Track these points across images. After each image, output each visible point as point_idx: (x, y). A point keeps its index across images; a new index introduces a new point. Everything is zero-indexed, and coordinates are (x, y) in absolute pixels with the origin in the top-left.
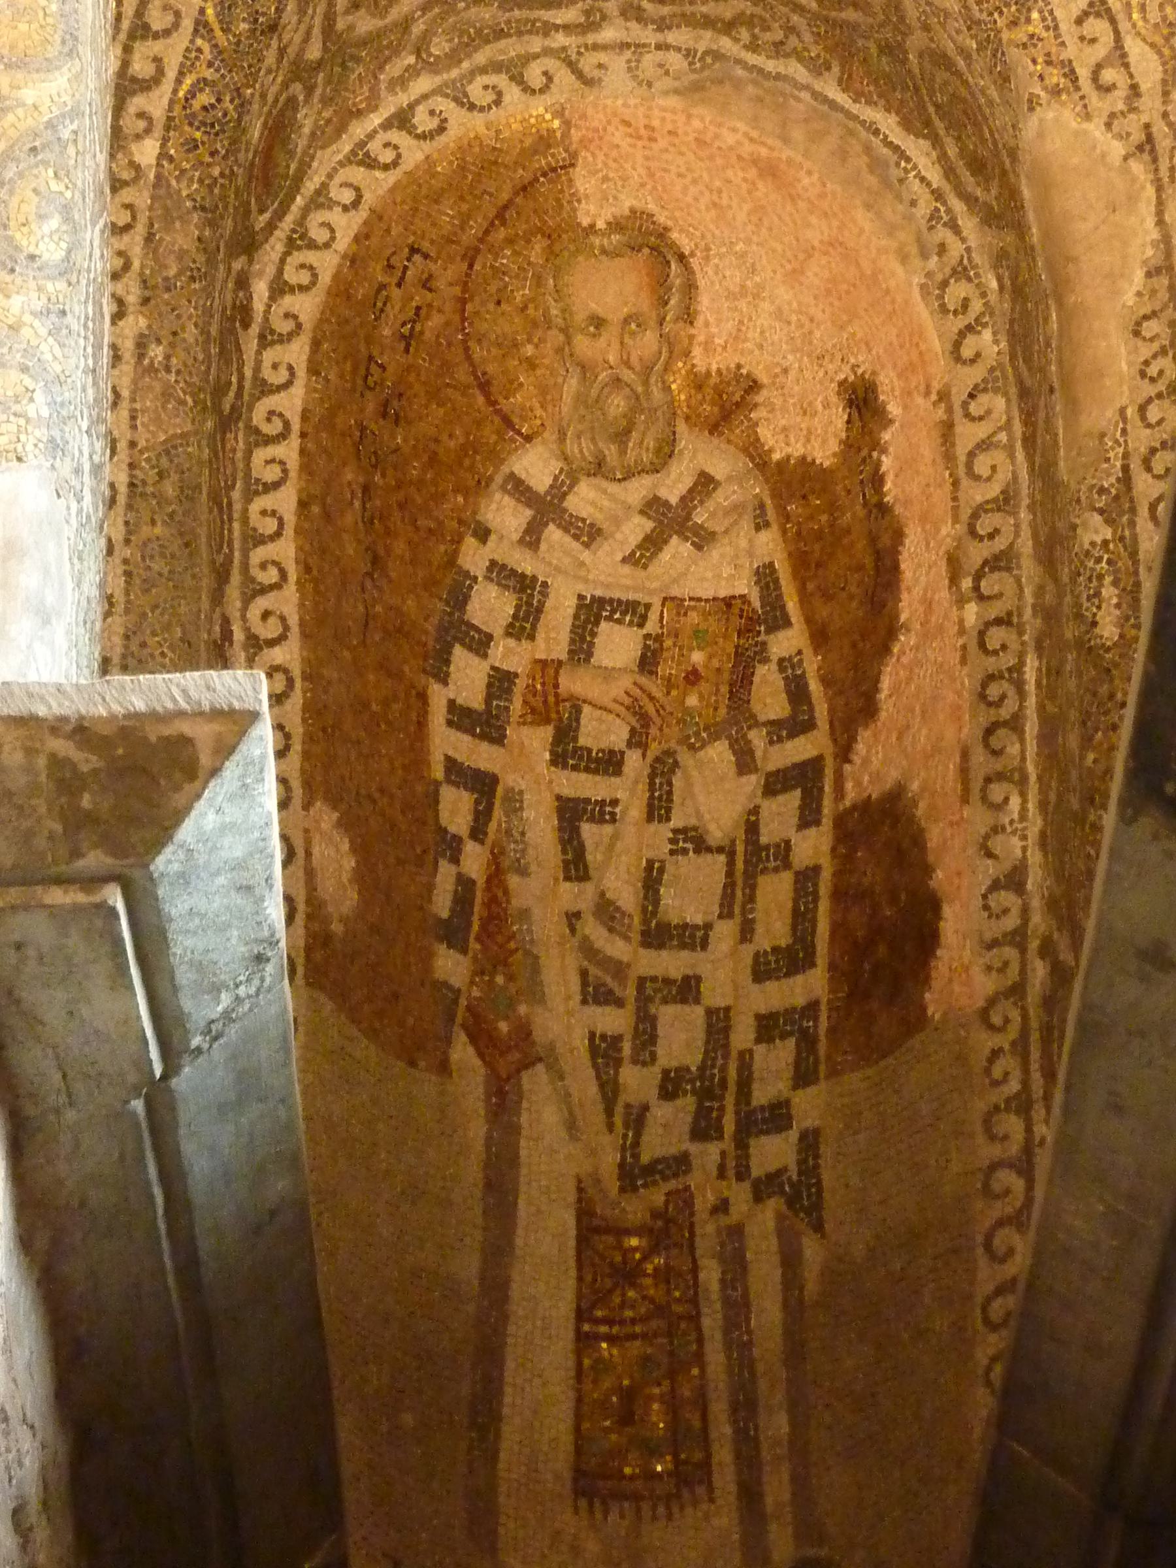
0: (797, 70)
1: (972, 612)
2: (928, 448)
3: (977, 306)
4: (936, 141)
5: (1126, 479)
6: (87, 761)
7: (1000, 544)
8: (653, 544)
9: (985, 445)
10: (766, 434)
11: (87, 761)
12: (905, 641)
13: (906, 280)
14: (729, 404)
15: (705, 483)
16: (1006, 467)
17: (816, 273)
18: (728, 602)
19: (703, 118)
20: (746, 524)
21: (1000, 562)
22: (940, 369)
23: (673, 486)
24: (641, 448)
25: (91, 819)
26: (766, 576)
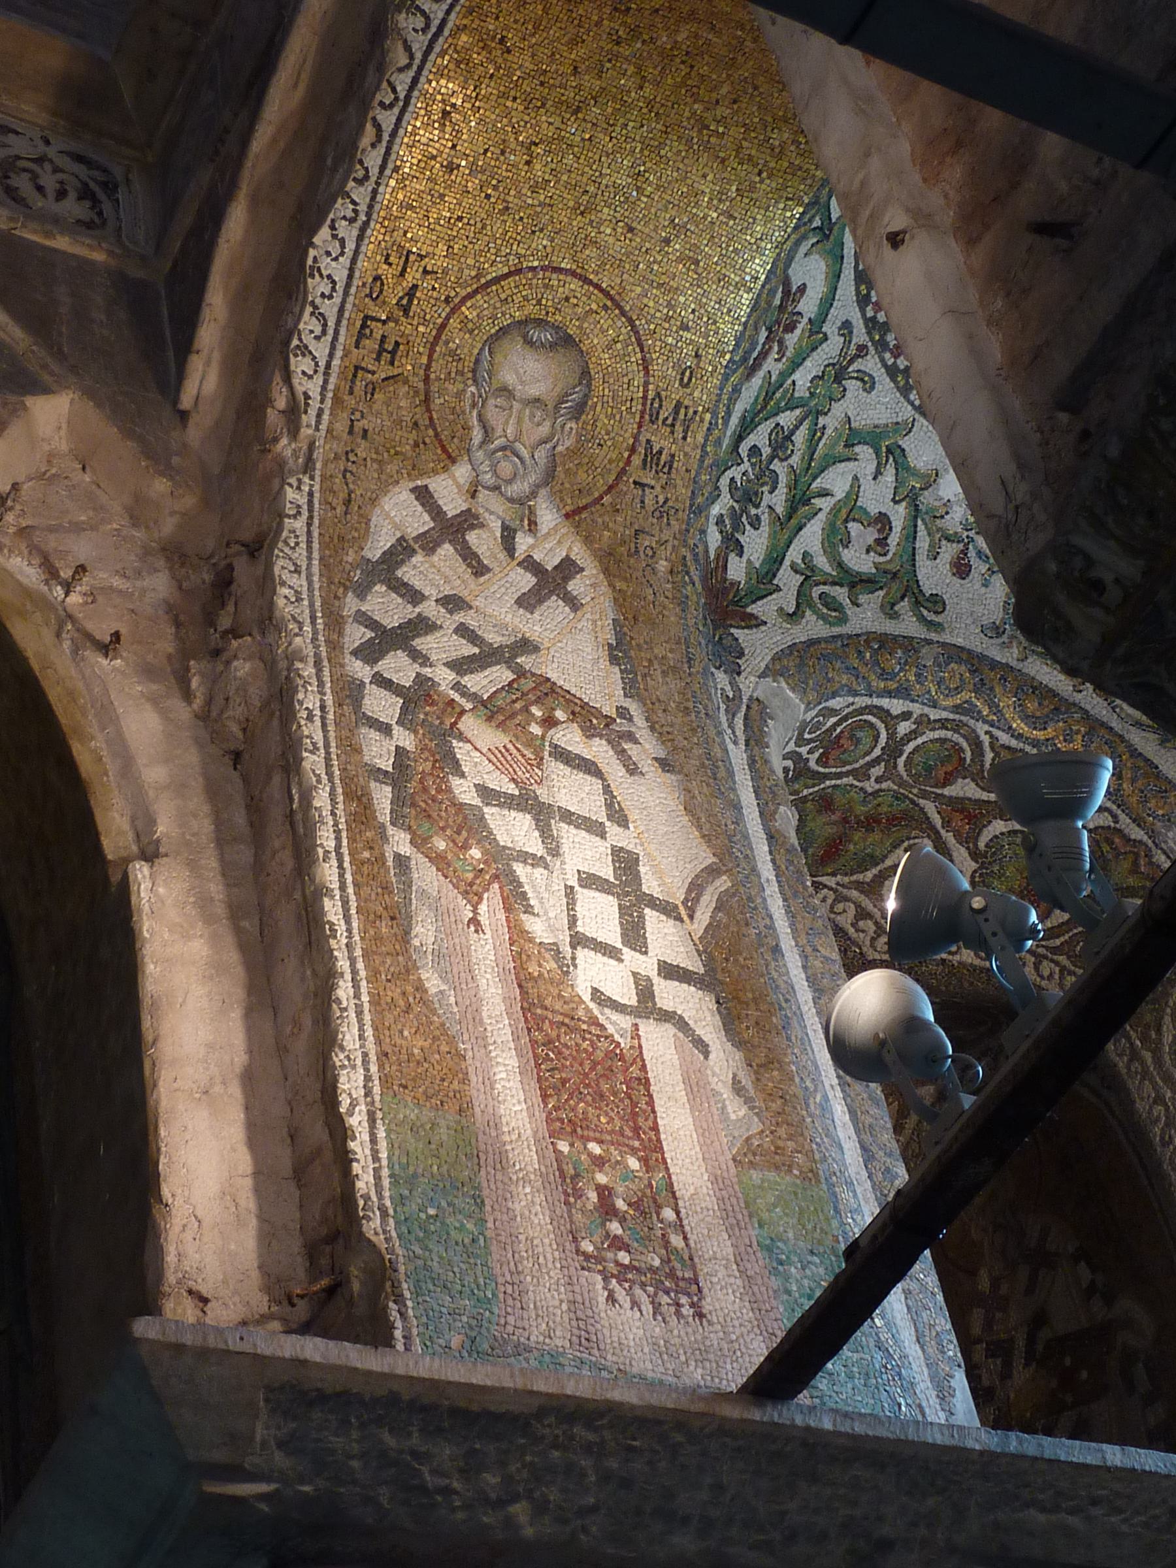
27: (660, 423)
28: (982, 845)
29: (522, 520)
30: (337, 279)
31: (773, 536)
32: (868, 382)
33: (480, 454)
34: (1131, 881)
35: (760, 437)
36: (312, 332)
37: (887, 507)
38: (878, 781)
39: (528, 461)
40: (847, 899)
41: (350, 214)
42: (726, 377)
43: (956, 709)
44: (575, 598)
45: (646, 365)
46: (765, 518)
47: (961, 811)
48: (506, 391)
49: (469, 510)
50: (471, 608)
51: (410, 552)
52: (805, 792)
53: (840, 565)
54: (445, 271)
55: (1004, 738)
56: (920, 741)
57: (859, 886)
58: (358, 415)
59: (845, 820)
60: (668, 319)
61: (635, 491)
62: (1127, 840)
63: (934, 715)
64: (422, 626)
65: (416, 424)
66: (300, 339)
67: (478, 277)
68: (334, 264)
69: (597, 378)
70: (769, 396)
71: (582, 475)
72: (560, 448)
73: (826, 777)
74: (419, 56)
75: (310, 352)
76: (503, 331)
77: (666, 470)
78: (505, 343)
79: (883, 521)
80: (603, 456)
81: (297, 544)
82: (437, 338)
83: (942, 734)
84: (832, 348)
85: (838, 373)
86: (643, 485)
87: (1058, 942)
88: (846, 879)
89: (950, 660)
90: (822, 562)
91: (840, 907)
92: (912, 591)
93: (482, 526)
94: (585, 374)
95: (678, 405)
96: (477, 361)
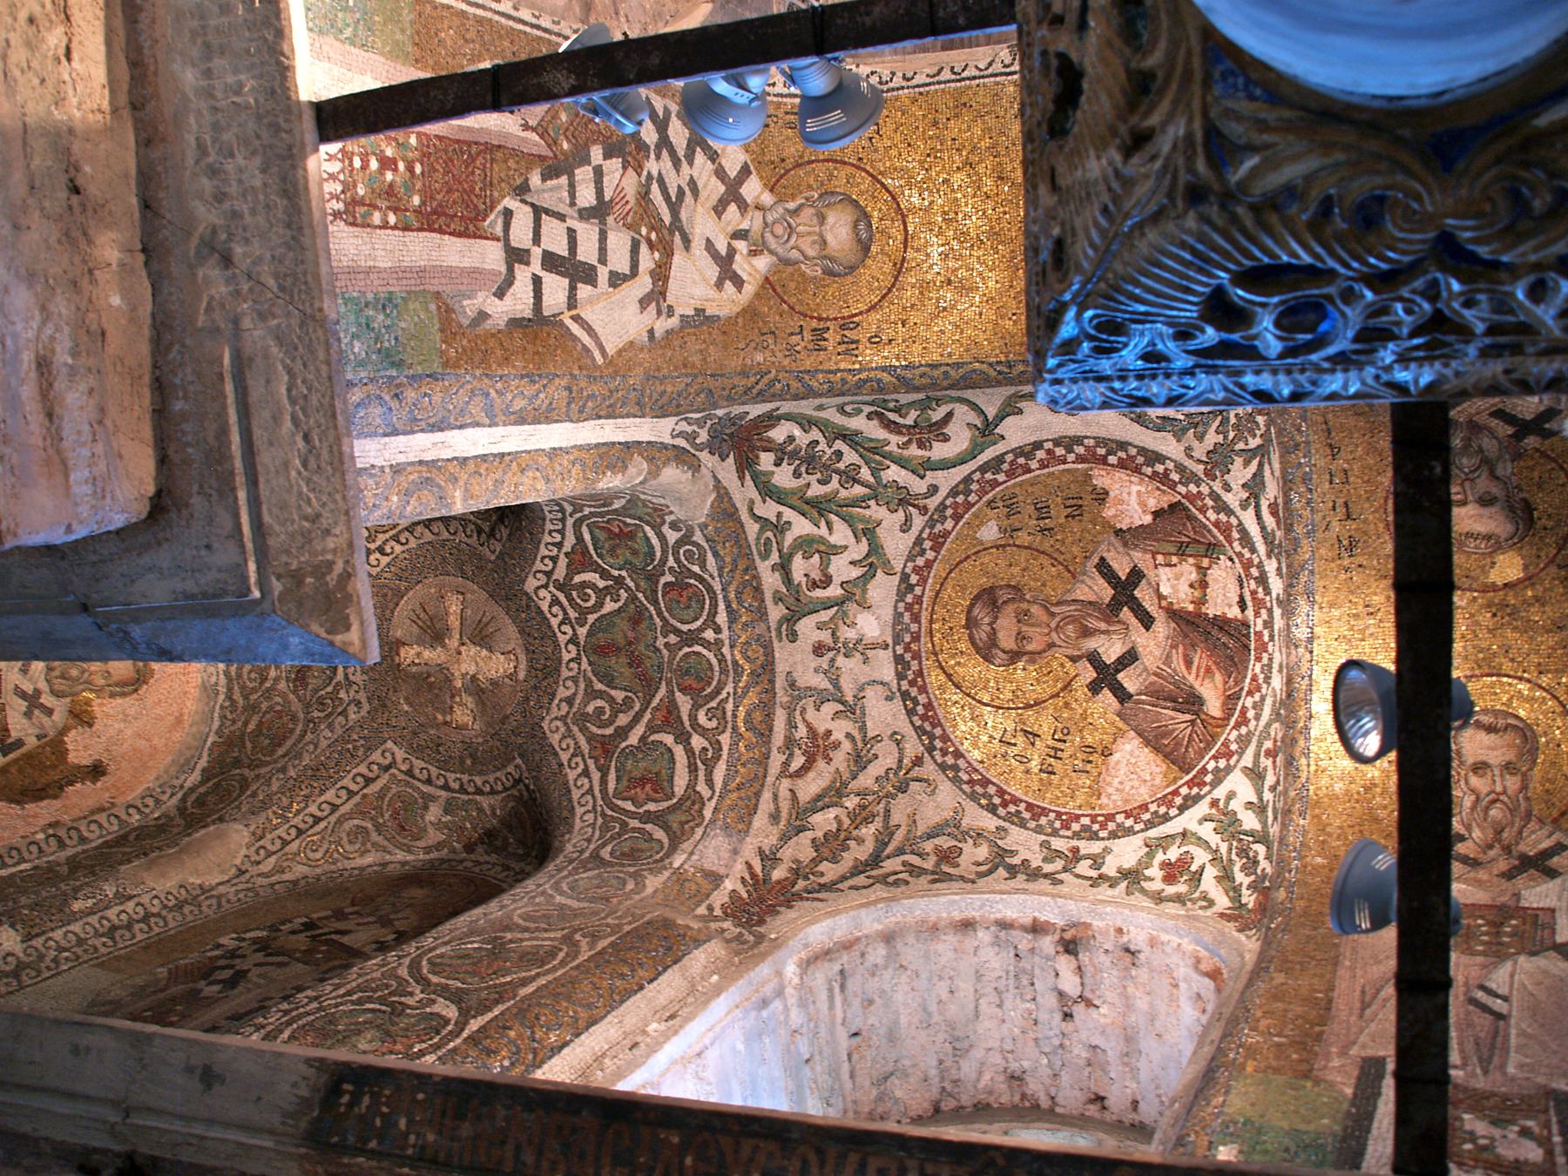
0: (216, 724)
1: (41, 836)
2: (91, 803)
3: (147, 811)
4: (202, 783)
5: (131, 898)
6: (332, 579)
7: (68, 841)
8: (23, 695)
9: (101, 826)
10: (73, 732)
11: (332, 579)
12: (16, 809)
13: (149, 781)
14: (81, 717)
15: (49, 712)
16: (95, 838)
17: (142, 744)
18: (7, 730)
19: (195, 692)
20: (37, 731)
21: (62, 844)
22: (120, 800)
23: (47, 700)
24: (60, 685)
25: (300, 583)
26: (19, 743)
28: (652, 738)
31: (793, 492)
32: (906, 526)
33: (781, 210)
34: (675, 825)
35: (850, 457)
37: (837, 580)
38: (667, 645)
40: (576, 683)
42: (884, 369)
43: (735, 663)
45: (872, 308)
46: (802, 482)
47: (669, 712)
48: (822, 219)
51: (713, 161)
52: (640, 595)
53: (791, 555)
54: (876, 151)
55: (730, 706)
56: (705, 652)
57: (589, 684)
59: (630, 644)
60: (904, 308)
62: (700, 811)
63: (726, 650)
65: (783, 160)
67: (881, 173)
69: (850, 279)
70: (874, 451)
71: (793, 285)
73: (655, 603)
74: (990, 71)
76: (855, 203)
78: (850, 209)
79: (827, 581)
80: (807, 297)
82: (836, 161)
83: (714, 661)
84: (919, 486)
85: (903, 500)
86: (801, 332)
87: (610, 813)
88: (590, 674)
89: (765, 647)
90: (789, 538)
91: (569, 683)
92: (792, 619)
94: (852, 269)
95: (857, 342)
96: (832, 193)
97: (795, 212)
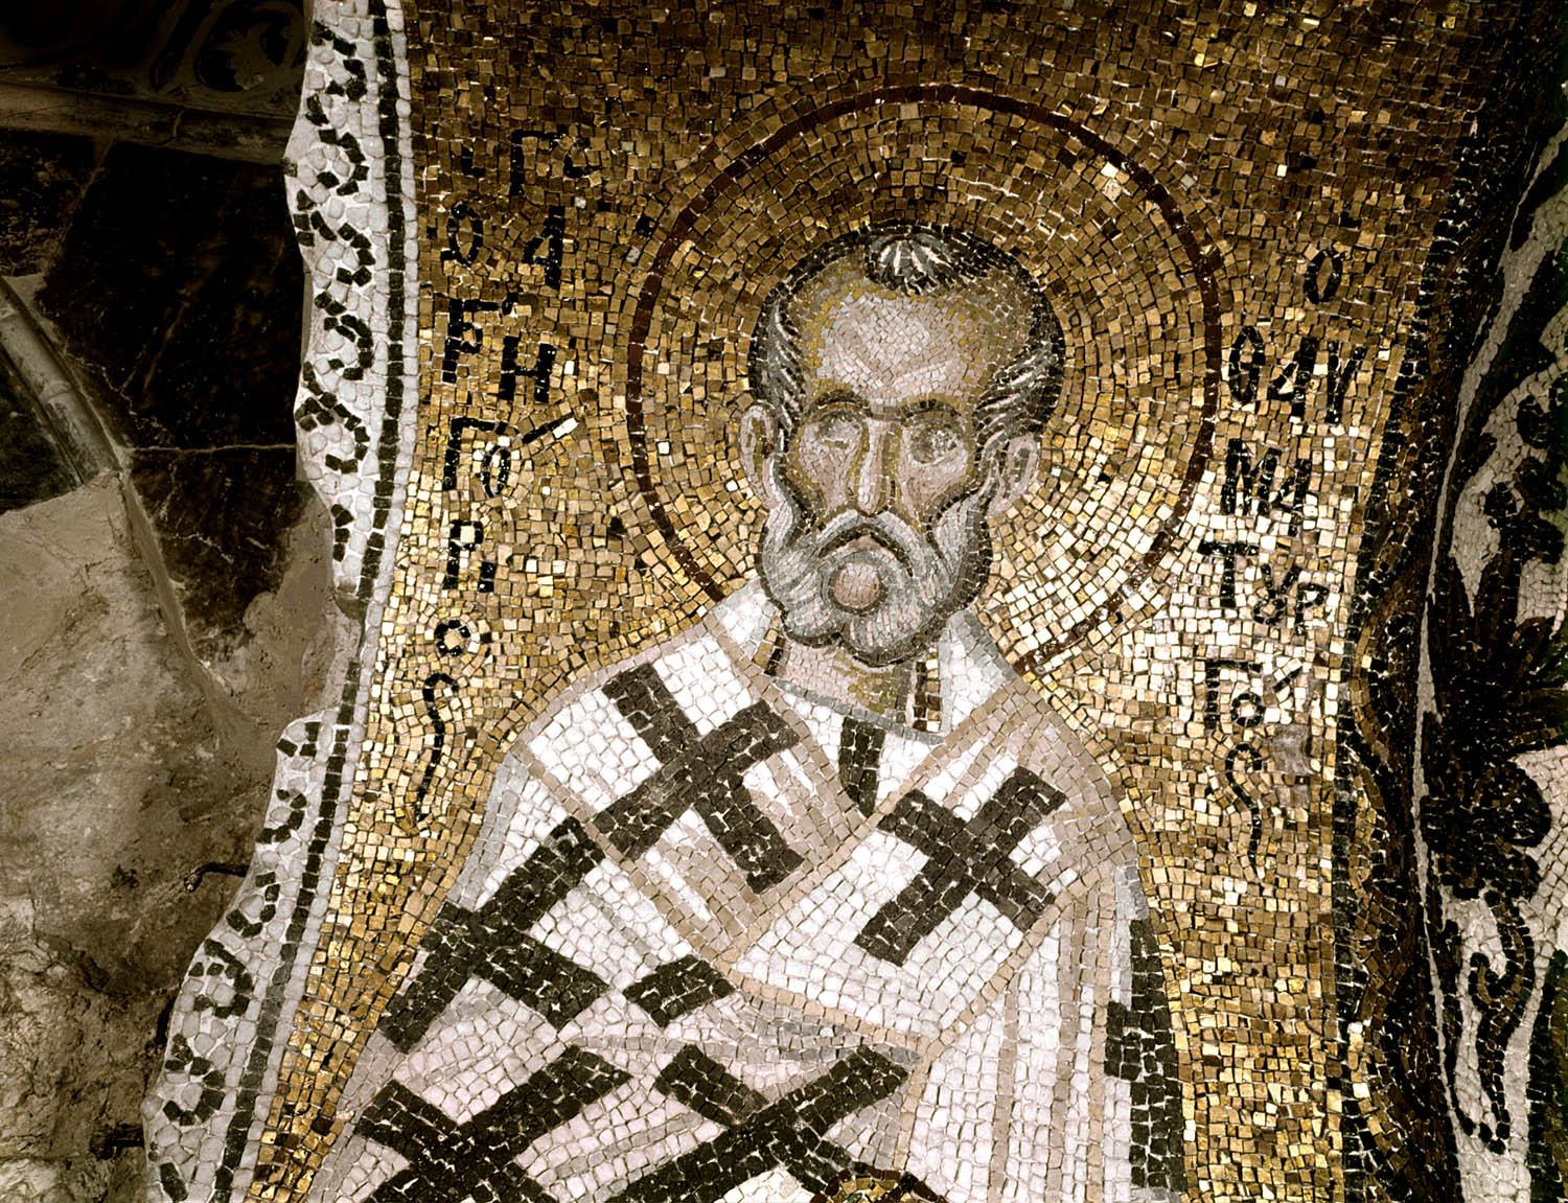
27: (1262, 394)
29: (899, 703)
30: (367, 233)
36: (335, 364)
39: (919, 553)
41: (343, 76)
44: (1034, 883)
48: (841, 402)
49: (762, 705)
50: (723, 989)
58: (468, 534)
61: (1206, 569)
64: (565, 1088)
66: (314, 387)
68: (348, 199)
72: (997, 506)
75: (343, 412)
77: (1290, 498)
81: (268, 914)
93: (791, 740)
97: (803, 504)
